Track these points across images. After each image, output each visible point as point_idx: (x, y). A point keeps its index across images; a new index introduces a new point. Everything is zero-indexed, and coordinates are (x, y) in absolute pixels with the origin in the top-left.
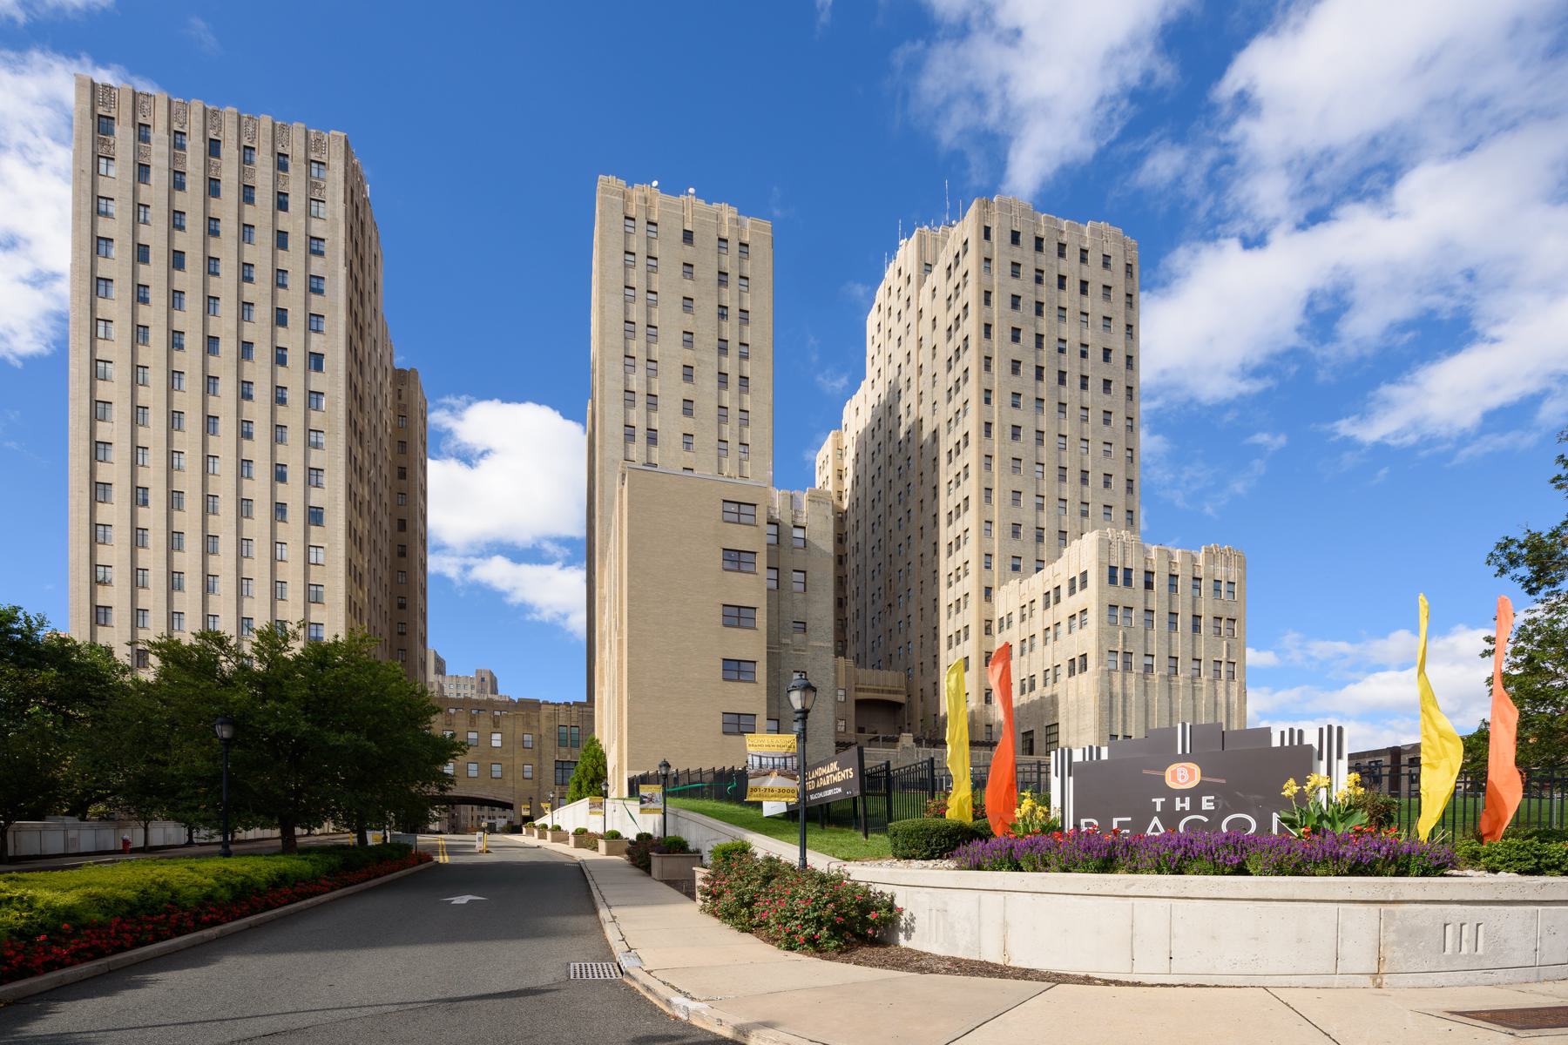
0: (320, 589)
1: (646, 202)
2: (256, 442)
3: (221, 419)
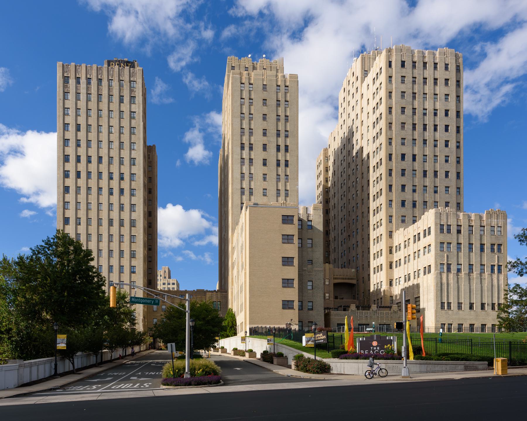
0: (135, 252)
1: (248, 76)
2: (114, 196)
3: (103, 188)
